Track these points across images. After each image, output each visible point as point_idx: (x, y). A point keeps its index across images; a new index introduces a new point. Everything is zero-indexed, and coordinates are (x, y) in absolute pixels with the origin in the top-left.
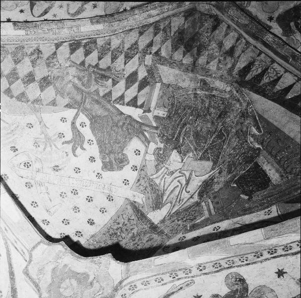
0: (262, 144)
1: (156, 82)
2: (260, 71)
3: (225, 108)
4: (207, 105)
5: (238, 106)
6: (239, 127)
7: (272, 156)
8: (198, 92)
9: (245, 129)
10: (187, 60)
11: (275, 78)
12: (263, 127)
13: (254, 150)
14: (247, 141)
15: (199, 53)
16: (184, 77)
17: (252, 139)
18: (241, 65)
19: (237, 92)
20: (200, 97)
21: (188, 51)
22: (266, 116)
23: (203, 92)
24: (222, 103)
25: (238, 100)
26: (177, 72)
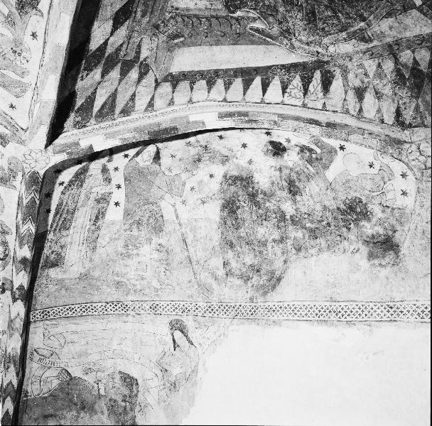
0: (237, 19)
1: (423, 4)
2: (311, 88)
3: (316, 26)
4: (340, 15)
5: (303, 38)
6: (279, 16)
7: (213, 17)
8: (362, 24)
9: (271, 19)
10: (406, 56)
11: (288, 90)
12: (253, 36)
13: (237, 8)
14: (255, 9)
15: (398, 72)
16: (394, 33)
17: (251, 15)
18: (337, 85)
19: (318, 53)
20: (355, 20)
21: (413, 69)
22: (261, 47)
23: (356, 28)
24: (323, 29)
25: (308, 44)
26: (408, 34)
